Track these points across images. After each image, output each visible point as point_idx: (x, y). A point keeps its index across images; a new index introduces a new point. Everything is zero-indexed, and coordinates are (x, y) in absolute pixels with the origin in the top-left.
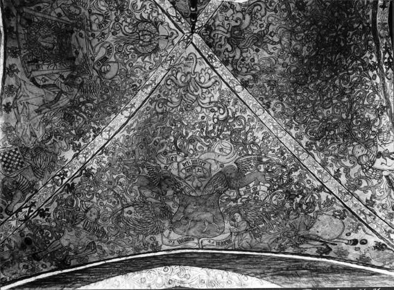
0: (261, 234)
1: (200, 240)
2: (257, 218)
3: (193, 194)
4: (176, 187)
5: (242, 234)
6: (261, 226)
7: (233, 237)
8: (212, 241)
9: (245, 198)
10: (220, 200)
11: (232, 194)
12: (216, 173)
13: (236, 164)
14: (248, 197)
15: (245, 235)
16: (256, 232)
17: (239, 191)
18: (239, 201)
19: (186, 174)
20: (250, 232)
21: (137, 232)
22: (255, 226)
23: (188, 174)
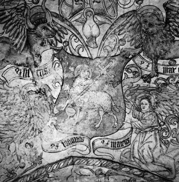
0: (169, 139)
1: (92, 141)
2: (171, 112)
3: (84, 54)
4: (56, 40)
5: (146, 132)
6: (172, 127)
7: (134, 135)
8: (106, 141)
9: (163, 79)
10: (124, 72)
11: (144, 66)
12: (126, 11)
13: (168, 10)
14: (168, 79)
15: (148, 135)
16: (164, 134)
17: (156, 63)
18: (153, 80)
19: (72, 7)
20: (157, 132)
21: (6, 140)
22: (164, 124)
23: (76, 7)
